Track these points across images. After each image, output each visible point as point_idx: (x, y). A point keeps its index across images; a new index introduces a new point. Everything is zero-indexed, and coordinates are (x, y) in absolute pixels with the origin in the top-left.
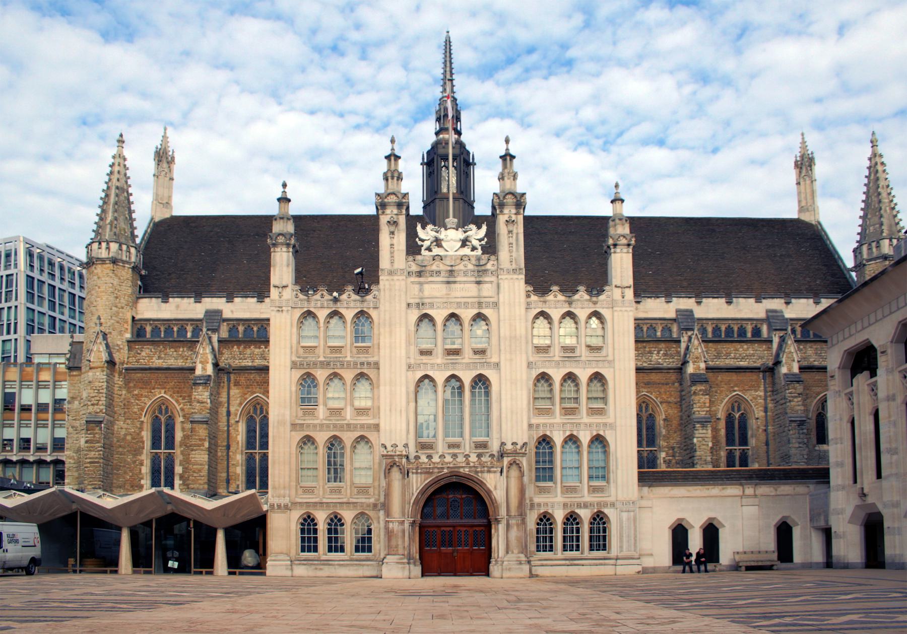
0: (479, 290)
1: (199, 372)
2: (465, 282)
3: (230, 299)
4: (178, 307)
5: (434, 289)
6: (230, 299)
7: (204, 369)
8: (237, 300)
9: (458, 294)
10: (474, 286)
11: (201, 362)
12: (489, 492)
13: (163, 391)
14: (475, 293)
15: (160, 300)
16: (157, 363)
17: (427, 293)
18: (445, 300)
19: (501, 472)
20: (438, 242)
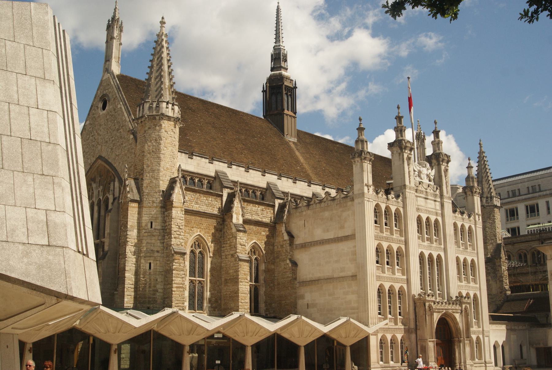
0: (435, 205)
1: (234, 220)
2: (431, 200)
3: (230, 165)
4: (198, 164)
5: (421, 202)
6: (230, 165)
7: (238, 219)
8: (234, 167)
9: (429, 206)
10: (433, 202)
11: (236, 213)
12: (456, 323)
13: (199, 230)
14: (433, 207)
15: (187, 156)
16: (196, 207)
17: (419, 203)
18: (425, 209)
19: (461, 313)
20: (420, 172)
